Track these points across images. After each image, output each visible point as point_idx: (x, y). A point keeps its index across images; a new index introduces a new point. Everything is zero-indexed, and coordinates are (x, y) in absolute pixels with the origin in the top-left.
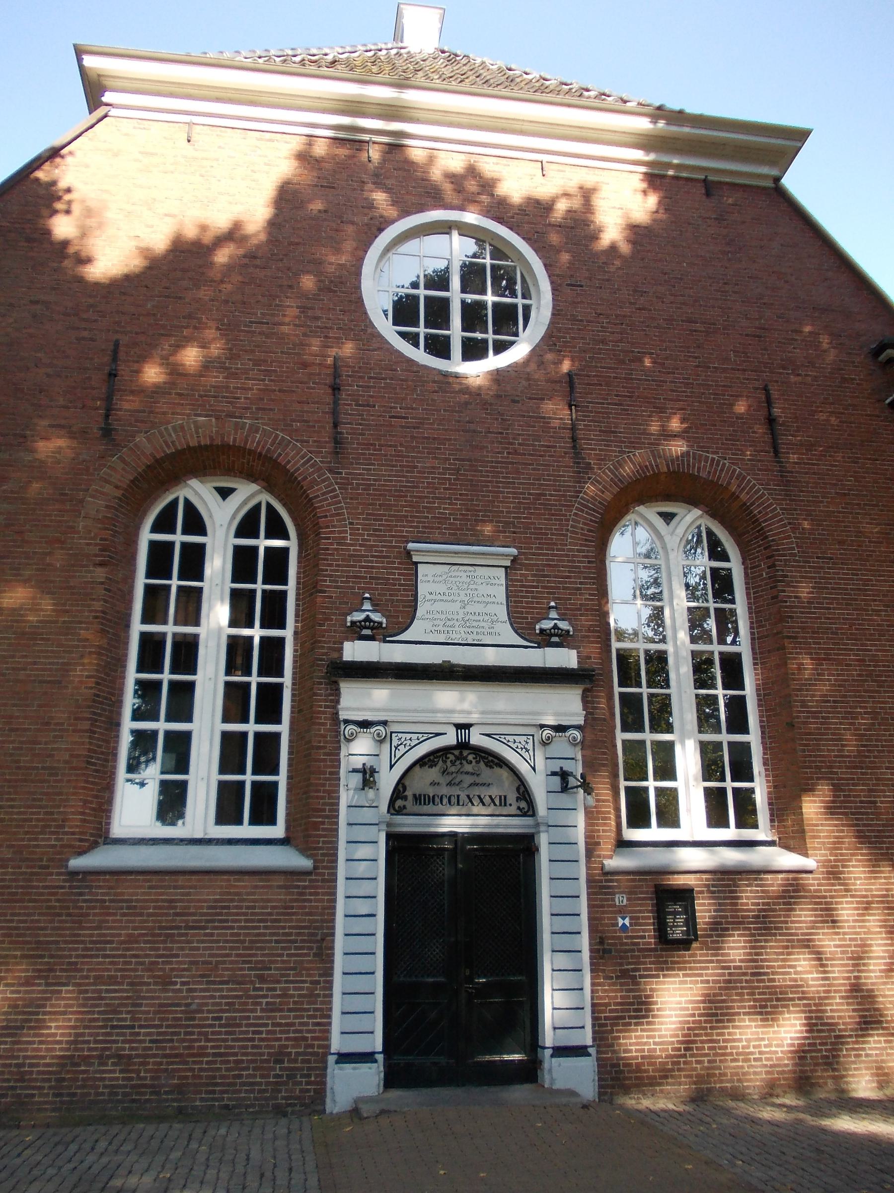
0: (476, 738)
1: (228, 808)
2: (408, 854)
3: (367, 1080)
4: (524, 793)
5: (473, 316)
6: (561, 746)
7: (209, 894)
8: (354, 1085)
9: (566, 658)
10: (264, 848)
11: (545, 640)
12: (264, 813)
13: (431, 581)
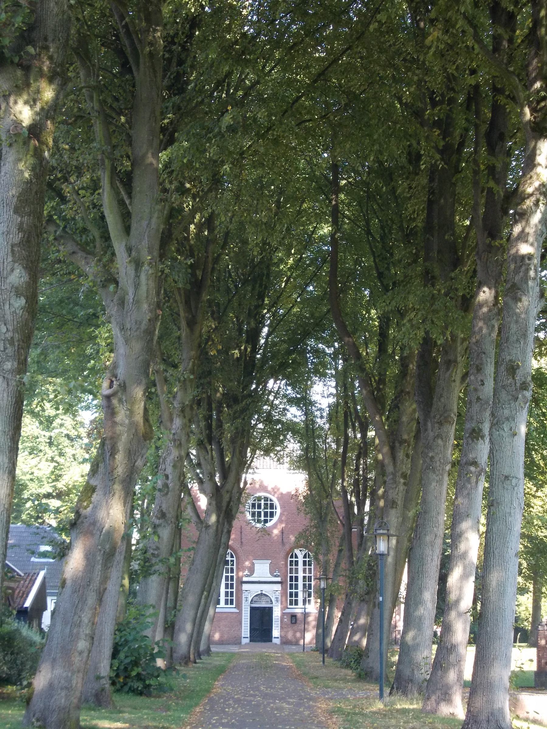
0: (264, 592)
1: (226, 602)
2: (253, 610)
3: (248, 640)
4: (271, 601)
5: (266, 514)
6: (277, 593)
7: (225, 615)
8: (245, 641)
9: (279, 579)
10: (232, 609)
11: (275, 576)
12: (232, 603)
13: (257, 567)
